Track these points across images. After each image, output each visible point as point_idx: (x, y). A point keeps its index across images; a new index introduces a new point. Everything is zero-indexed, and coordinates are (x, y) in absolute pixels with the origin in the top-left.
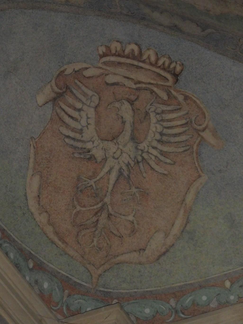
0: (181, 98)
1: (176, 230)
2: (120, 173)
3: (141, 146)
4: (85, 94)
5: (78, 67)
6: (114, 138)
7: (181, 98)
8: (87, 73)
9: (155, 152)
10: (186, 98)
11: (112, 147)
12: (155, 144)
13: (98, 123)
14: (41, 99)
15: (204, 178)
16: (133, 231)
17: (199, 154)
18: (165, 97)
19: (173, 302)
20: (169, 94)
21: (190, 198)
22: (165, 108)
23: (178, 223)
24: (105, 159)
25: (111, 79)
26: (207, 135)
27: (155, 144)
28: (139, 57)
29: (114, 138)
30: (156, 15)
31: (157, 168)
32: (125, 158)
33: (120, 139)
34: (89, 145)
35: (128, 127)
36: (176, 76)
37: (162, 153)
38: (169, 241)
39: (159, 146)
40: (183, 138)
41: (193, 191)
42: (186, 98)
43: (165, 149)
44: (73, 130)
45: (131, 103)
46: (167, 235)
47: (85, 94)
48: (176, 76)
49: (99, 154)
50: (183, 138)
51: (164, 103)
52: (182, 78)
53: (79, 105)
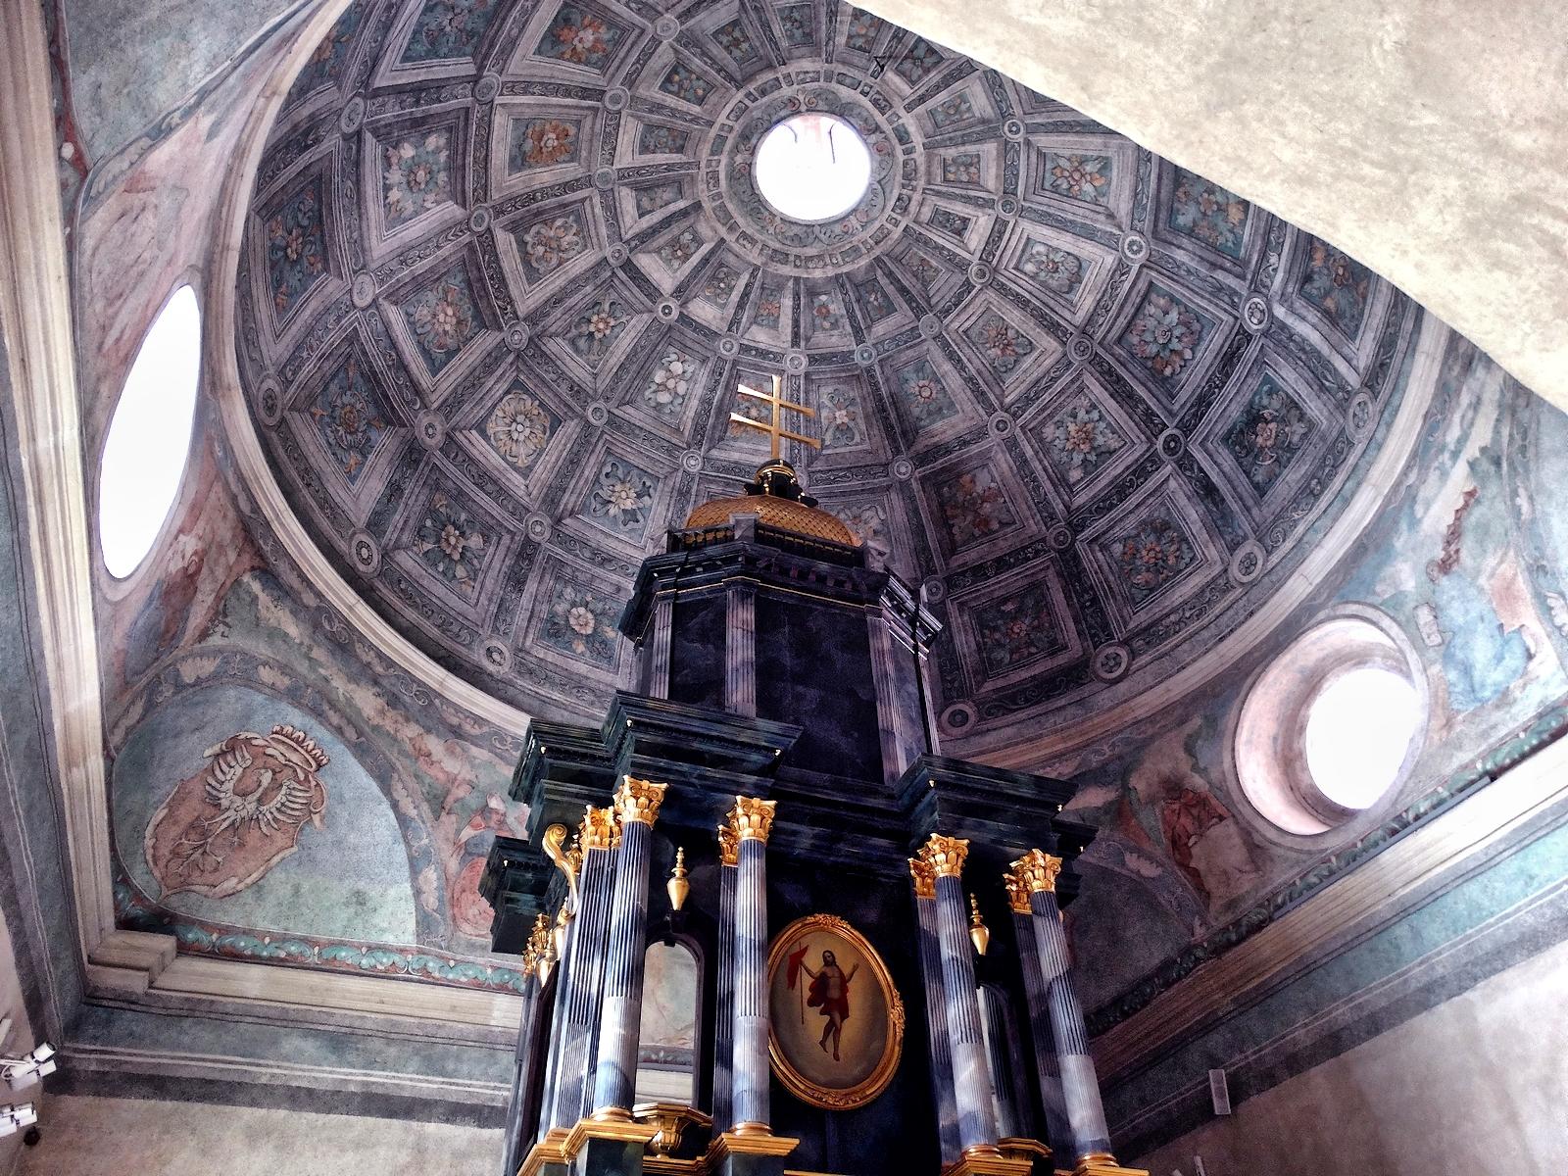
0: (313, 783)
1: (249, 881)
2: (233, 823)
3: (263, 808)
4: (243, 757)
5: (250, 735)
6: (244, 795)
7: (313, 783)
8: (254, 742)
9: (269, 816)
10: (318, 785)
11: (239, 801)
12: (273, 810)
13: (240, 780)
14: (208, 753)
15: (295, 849)
16: (216, 870)
17: (302, 829)
18: (302, 776)
19: (215, 936)
20: (306, 777)
21: (276, 859)
22: (297, 786)
23: (255, 876)
24: (227, 809)
25: (269, 751)
26: (316, 818)
27: (273, 810)
28: (300, 743)
29: (244, 795)
30: (331, 713)
31: (264, 829)
32: (244, 813)
33: (249, 798)
34: (222, 795)
35: (261, 790)
36: (319, 766)
37: (275, 819)
38: (241, 886)
39: (276, 814)
40: (297, 813)
41: (281, 855)
42: (318, 785)
43: (279, 816)
44: (217, 781)
45: (274, 773)
46: (240, 882)
47: (243, 757)
48: (319, 766)
49: (225, 803)
50: (297, 813)
51: (299, 782)
52: (322, 770)
53: (233, 763)
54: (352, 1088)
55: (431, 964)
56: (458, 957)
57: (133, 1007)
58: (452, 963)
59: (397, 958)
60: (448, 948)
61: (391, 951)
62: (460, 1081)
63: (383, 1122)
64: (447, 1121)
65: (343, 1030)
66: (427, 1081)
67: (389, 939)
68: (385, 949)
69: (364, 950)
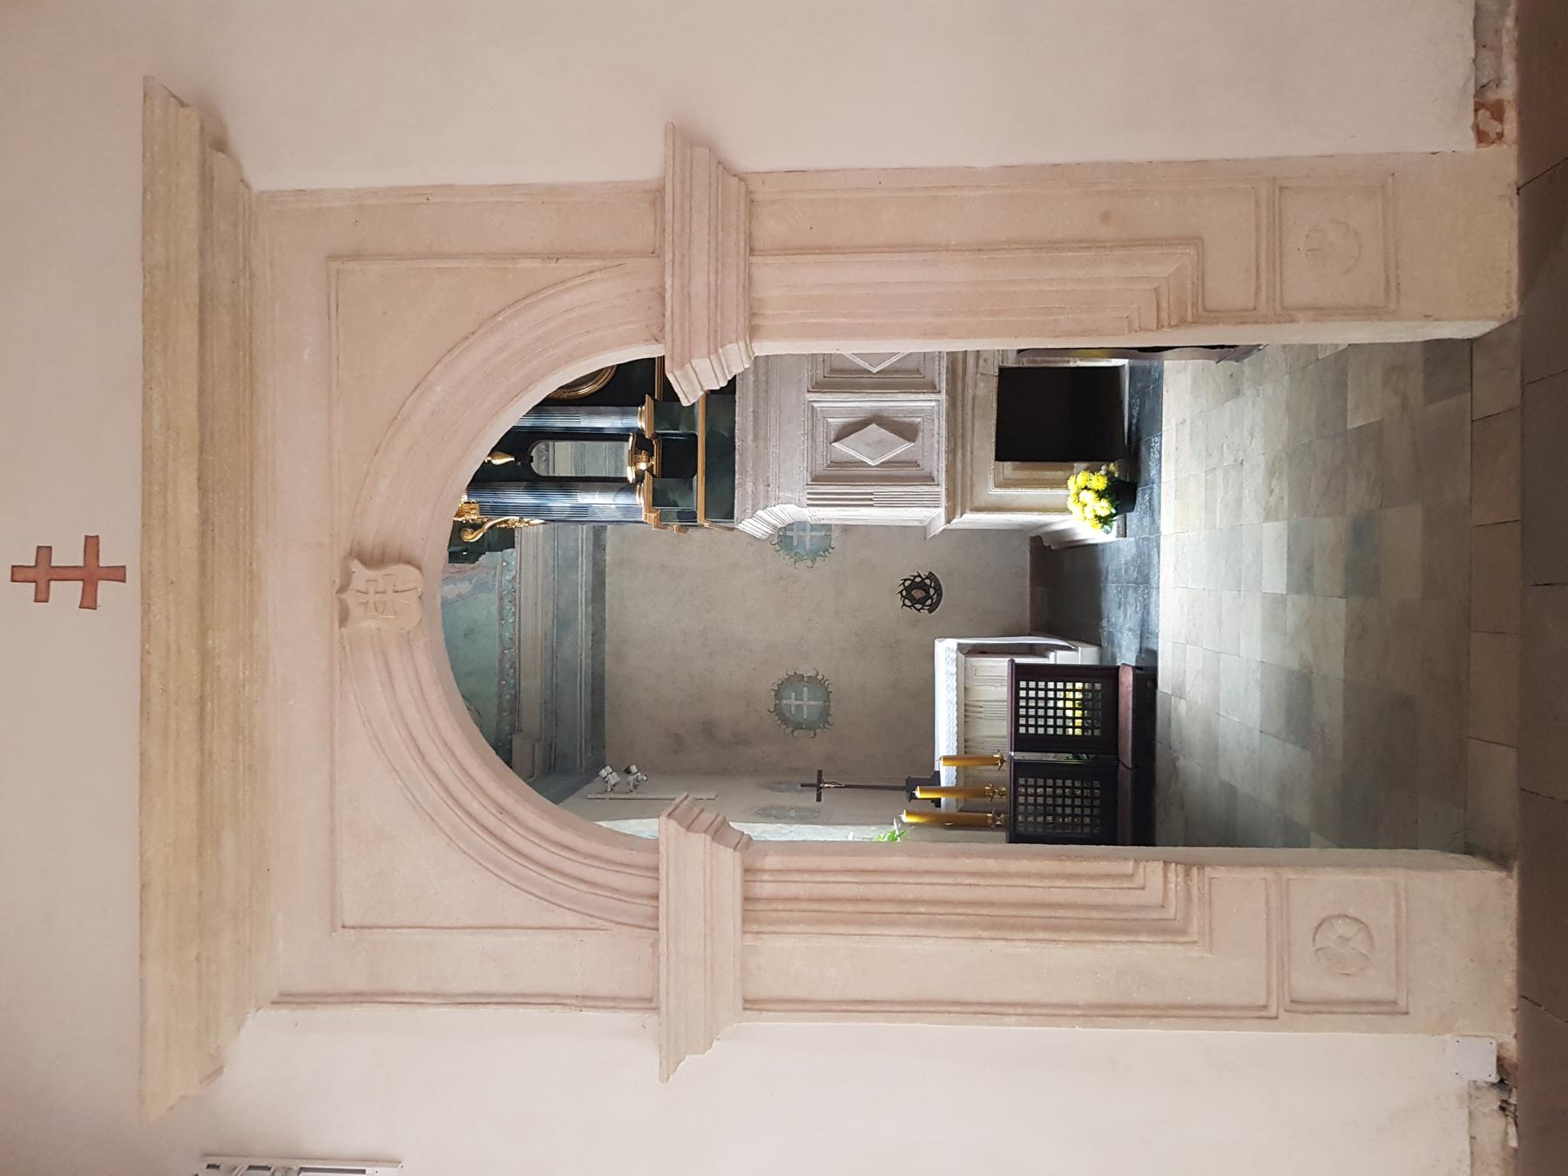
54: (590, 610)
55: (507, 578)
56: (500, 560)
57: (553, 746)
58: (505, 564)
59: (506, 601)
60: (495, 569)
61: (502, 605)
62: (580, 546)
63: (608, 588)
64: (604, 550)
65: (555, 622)
66: (582, 565)
67: (494, 609)
68: (501, 609)
69: (503, 622)
